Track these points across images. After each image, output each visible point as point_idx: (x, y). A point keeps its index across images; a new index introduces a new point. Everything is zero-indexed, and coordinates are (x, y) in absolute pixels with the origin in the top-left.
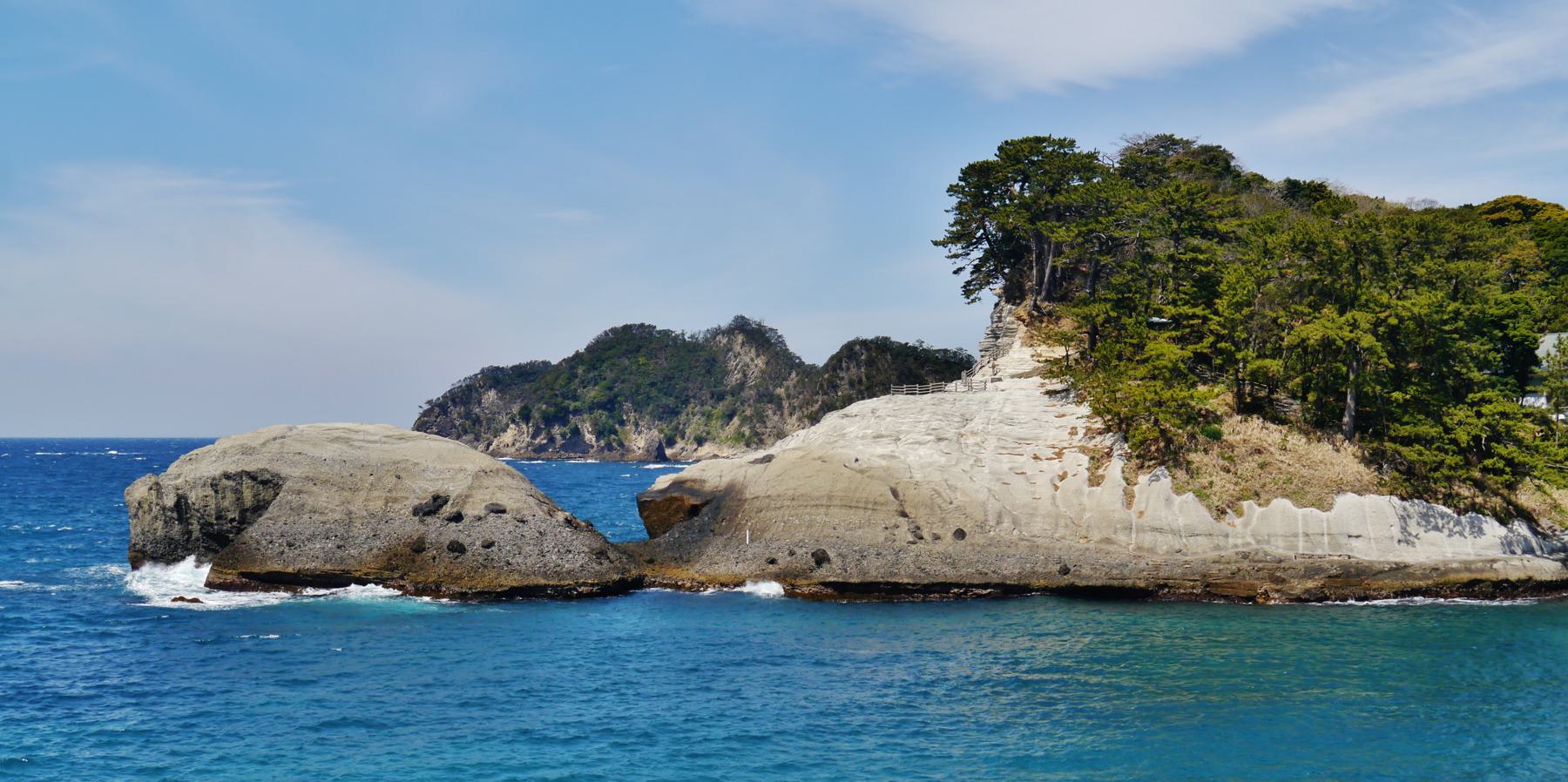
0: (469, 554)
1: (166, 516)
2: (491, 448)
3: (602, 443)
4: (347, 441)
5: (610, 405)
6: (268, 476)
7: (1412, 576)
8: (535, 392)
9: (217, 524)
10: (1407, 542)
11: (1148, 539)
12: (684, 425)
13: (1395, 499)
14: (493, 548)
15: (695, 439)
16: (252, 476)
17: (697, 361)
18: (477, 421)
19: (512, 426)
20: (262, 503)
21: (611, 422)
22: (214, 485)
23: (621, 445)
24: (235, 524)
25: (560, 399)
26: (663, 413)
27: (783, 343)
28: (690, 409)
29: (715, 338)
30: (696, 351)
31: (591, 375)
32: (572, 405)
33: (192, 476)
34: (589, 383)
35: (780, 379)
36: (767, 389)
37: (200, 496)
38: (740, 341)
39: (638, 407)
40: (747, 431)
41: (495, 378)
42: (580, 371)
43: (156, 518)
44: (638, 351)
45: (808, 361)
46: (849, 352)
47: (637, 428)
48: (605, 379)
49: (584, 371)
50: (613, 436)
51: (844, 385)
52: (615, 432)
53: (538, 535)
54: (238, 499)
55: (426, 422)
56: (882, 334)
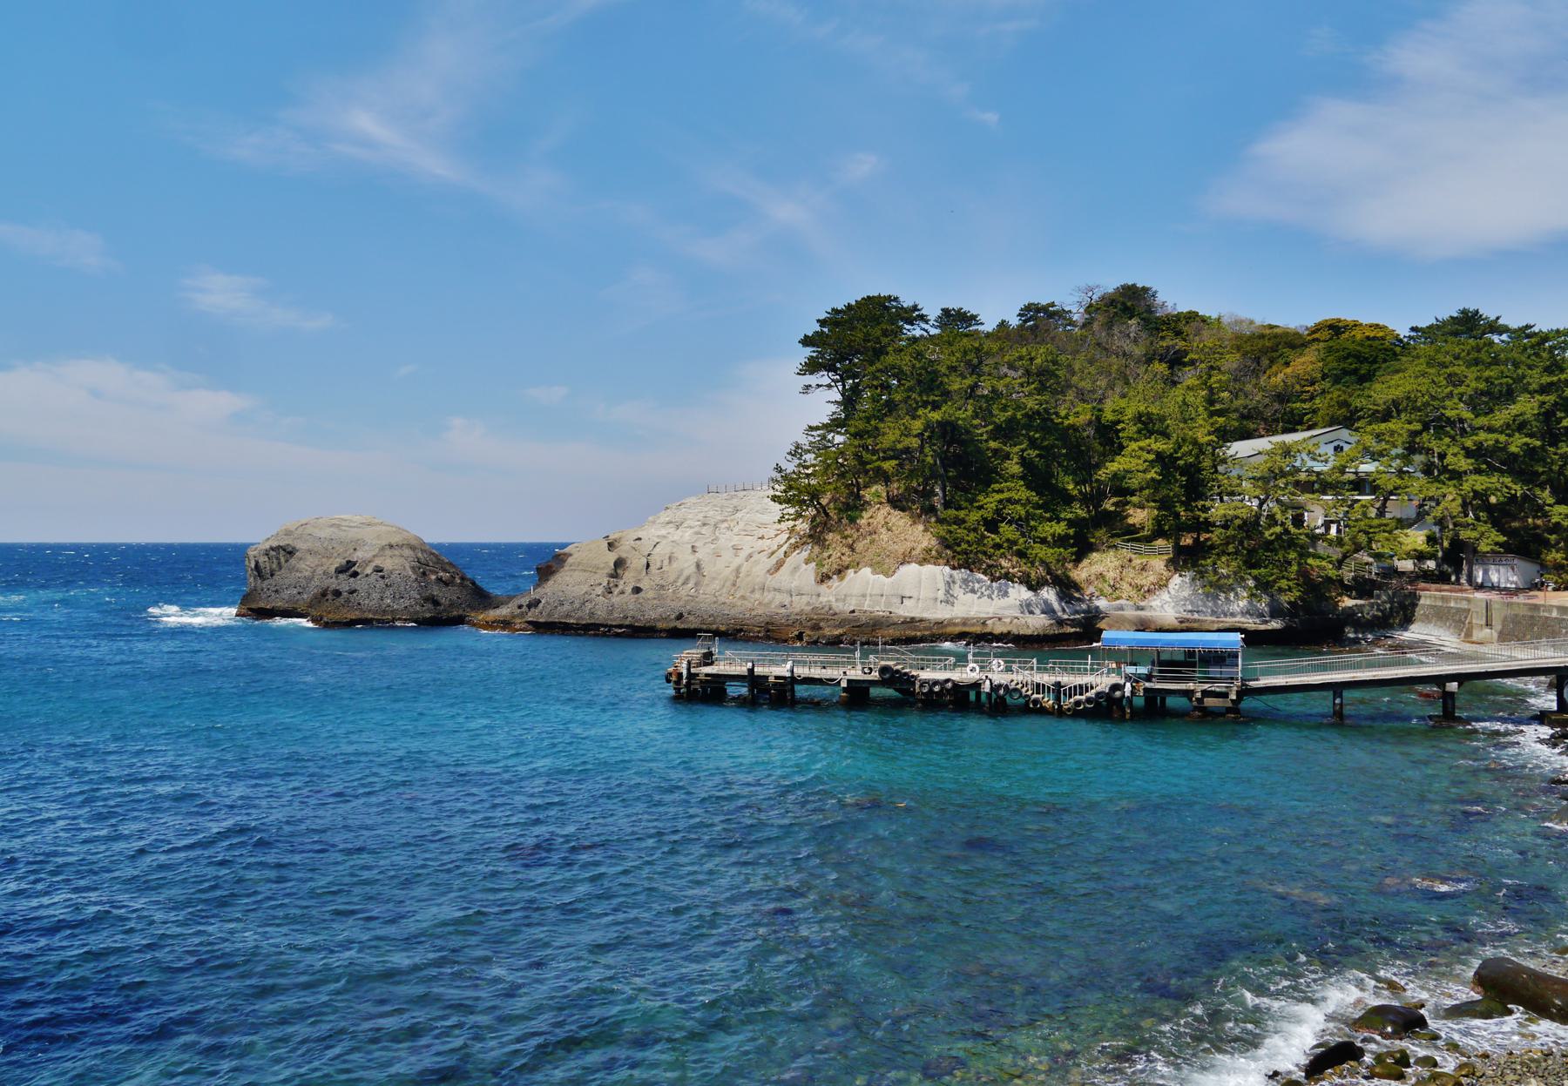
4: (338, 526)
7: (955, 625)
10: (947, 602)
11: (768, 596)
13: (947, 568)
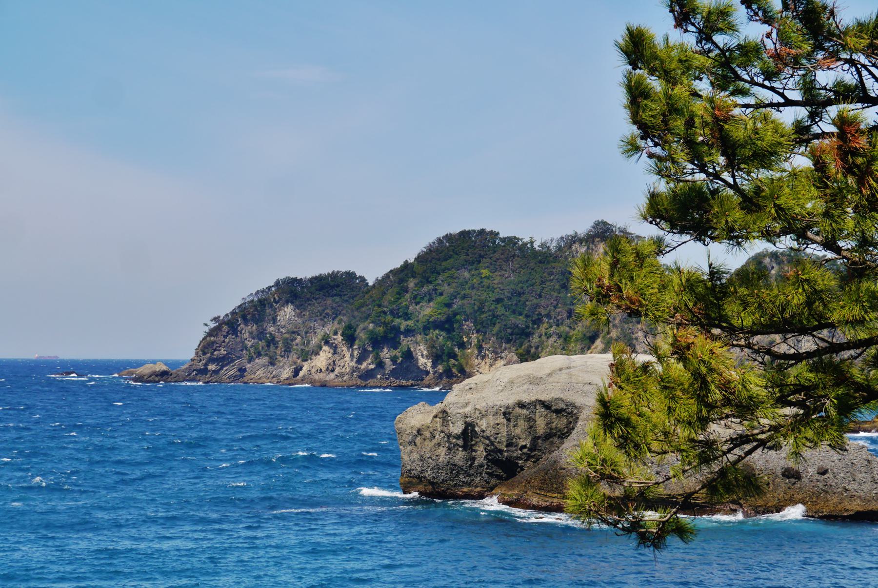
0: (805, 480)
1: (450, 443)
2: (301, 373)
3: (440, 368)
6: (562, 406)
8: (358, 309)
9: (507, 451)
12: (537, 348)
14: (825, 476)
16: (546, 405)
17: (551, 274)
18: (272, 341)
19: (325, 348)
20: (554, 431)
21: (449, 344)
22: (507, 414)
24: (525, 451)
26: (512, 334)
28: (543, 328)
29: (570, 247)
30: (548, 262)
31: (425, 289)
32: (404, 325)
33: (484, 404)
34: (422, 298)
37: (492, 423)
38: (601, 250)
39: (482, 328)
43: (439, 444)
44: (479, 262)
47: (480, 352)
48: (441, 294)
49: (416, 285)
50: (452, 361)
52: (455, 356)
53: (866, 463)
54: (531, 427)
55: (213, 343)
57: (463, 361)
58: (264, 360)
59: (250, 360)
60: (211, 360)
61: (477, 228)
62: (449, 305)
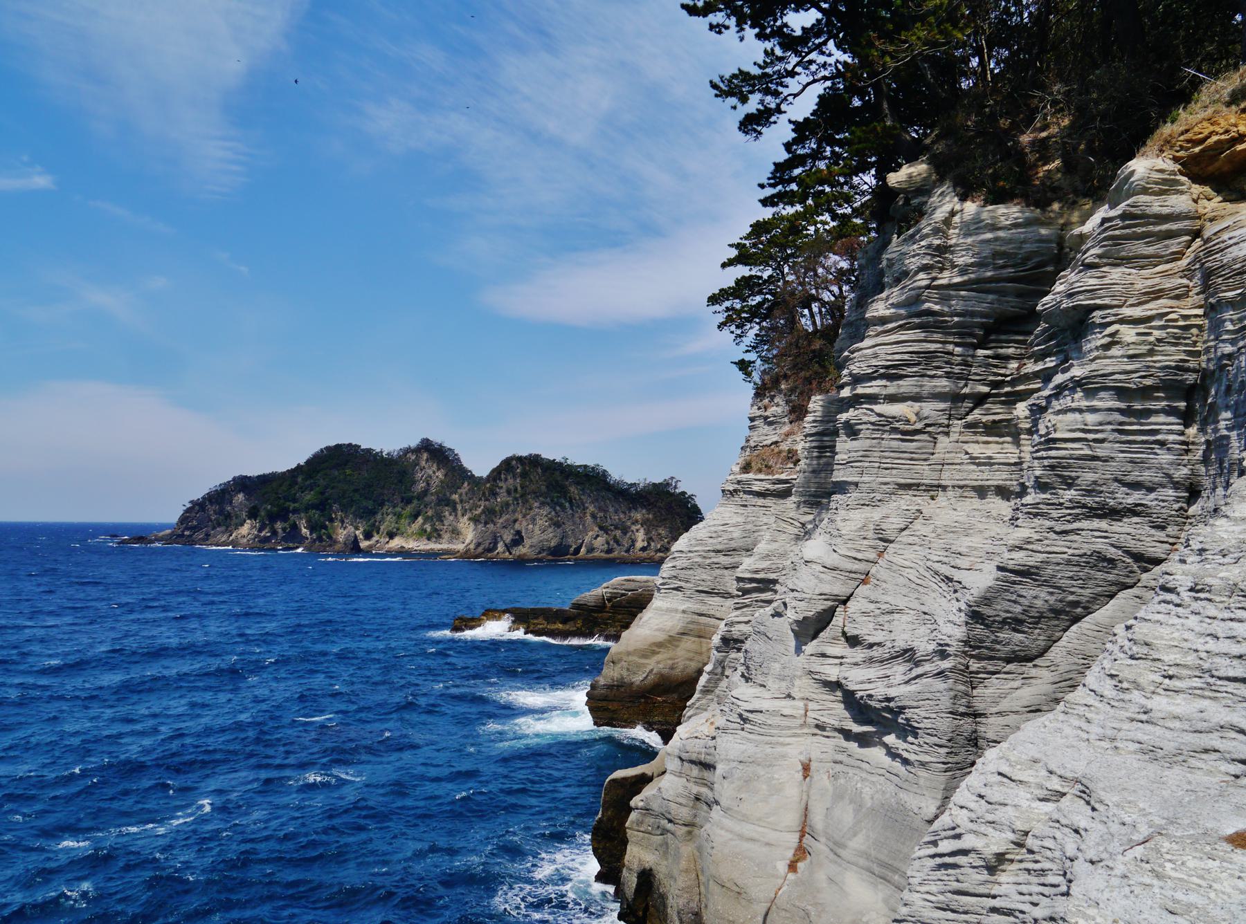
3: (314, 536)
5: (322, 506)
15: (387, 534)
18: (228, 516)
21: (322, 519)
23: (330, 537)
25: (282, 501)
27: (458, 460)
28: (385, 509)
31: (308, 482)
32: (292, 506)
35: (455, 488)
36: (445, 495)
39: (344, 508)
40: (428, 527)
41: (242, 484)
42: (300, 480)
44: (346, 465)
45: (477, 473)
46: (508, 466)
51: (503, 492)
52: (325, 527)
56: (534, 452)
57: (331, 531)
58: (223, 528)
59: (214, 528)
60: (187, 529)
61: (347, 442)
62: (322, 493)
